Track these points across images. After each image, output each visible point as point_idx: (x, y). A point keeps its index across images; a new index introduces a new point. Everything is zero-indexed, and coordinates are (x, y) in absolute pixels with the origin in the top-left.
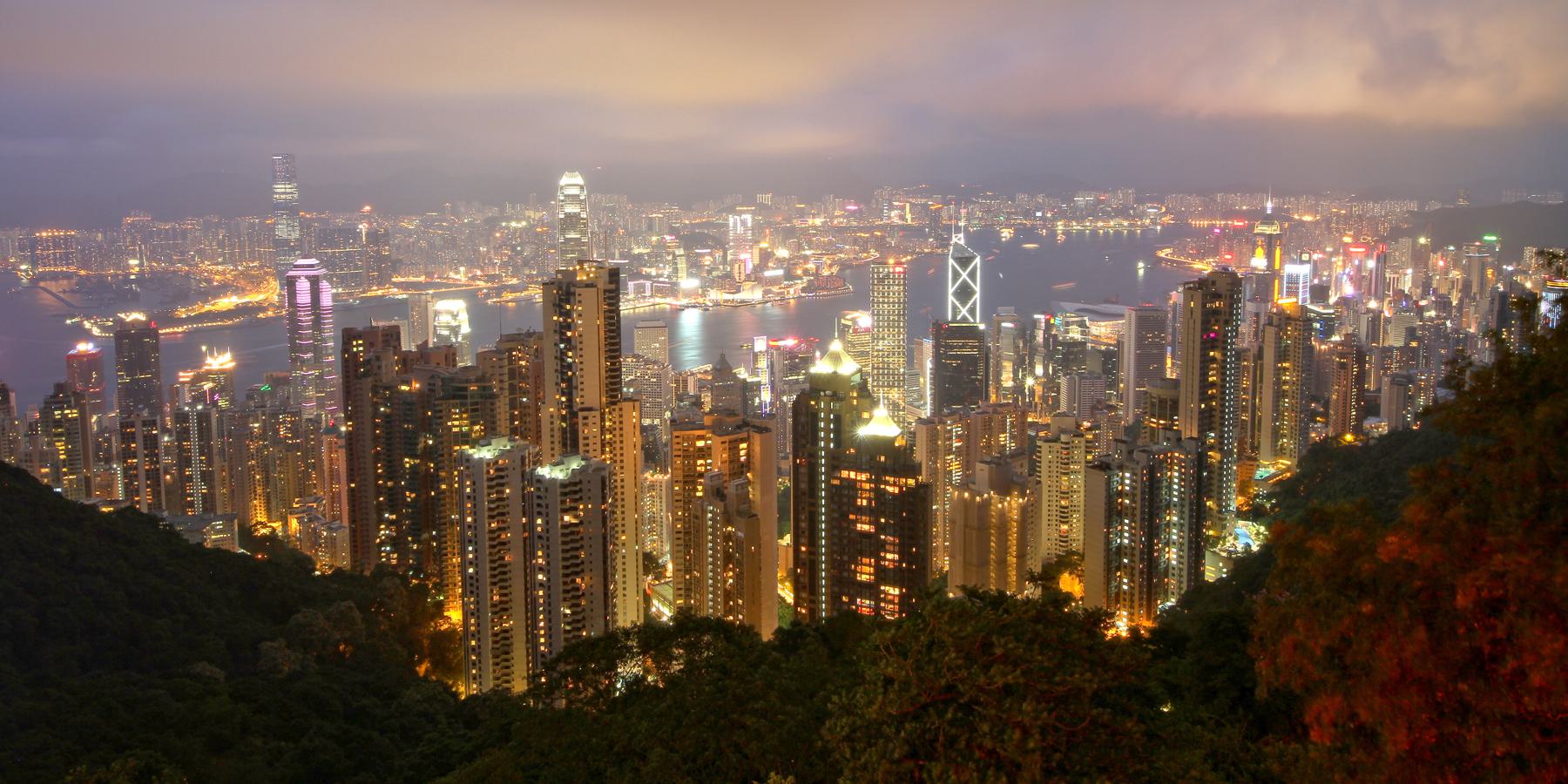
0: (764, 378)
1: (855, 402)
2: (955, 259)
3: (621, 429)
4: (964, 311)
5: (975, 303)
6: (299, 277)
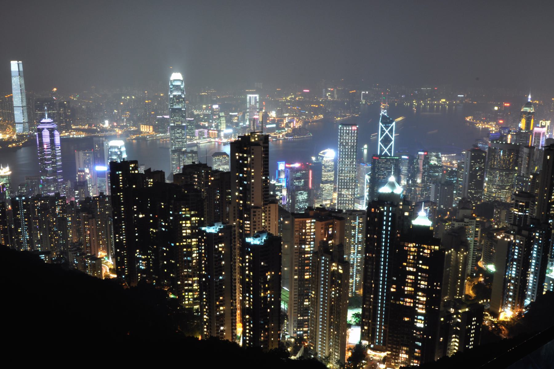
0: (284, 184)
1: (401, 207)
2: (381, 122)
3: (269, 217)
4: (386, 150)
5: (391, 146)
6: (43, 129)
